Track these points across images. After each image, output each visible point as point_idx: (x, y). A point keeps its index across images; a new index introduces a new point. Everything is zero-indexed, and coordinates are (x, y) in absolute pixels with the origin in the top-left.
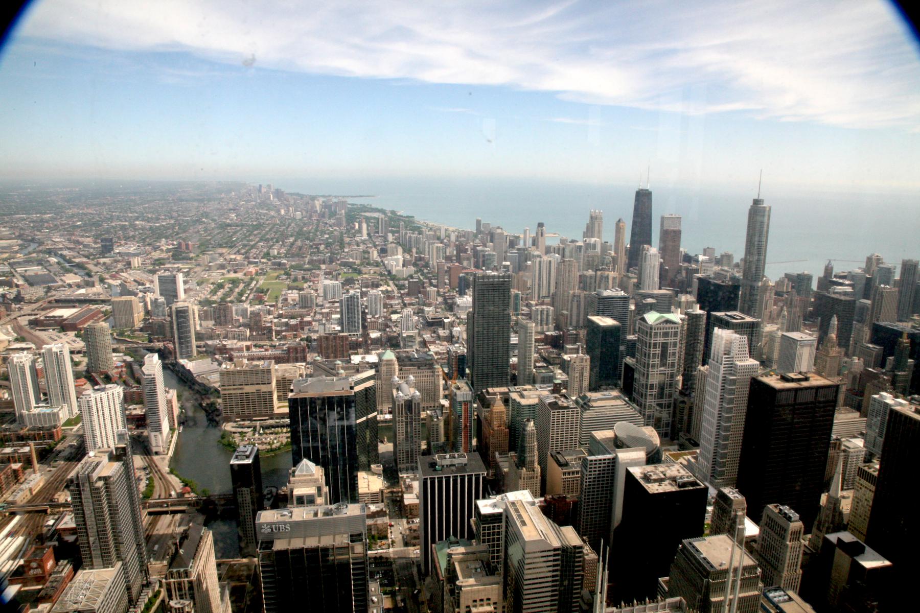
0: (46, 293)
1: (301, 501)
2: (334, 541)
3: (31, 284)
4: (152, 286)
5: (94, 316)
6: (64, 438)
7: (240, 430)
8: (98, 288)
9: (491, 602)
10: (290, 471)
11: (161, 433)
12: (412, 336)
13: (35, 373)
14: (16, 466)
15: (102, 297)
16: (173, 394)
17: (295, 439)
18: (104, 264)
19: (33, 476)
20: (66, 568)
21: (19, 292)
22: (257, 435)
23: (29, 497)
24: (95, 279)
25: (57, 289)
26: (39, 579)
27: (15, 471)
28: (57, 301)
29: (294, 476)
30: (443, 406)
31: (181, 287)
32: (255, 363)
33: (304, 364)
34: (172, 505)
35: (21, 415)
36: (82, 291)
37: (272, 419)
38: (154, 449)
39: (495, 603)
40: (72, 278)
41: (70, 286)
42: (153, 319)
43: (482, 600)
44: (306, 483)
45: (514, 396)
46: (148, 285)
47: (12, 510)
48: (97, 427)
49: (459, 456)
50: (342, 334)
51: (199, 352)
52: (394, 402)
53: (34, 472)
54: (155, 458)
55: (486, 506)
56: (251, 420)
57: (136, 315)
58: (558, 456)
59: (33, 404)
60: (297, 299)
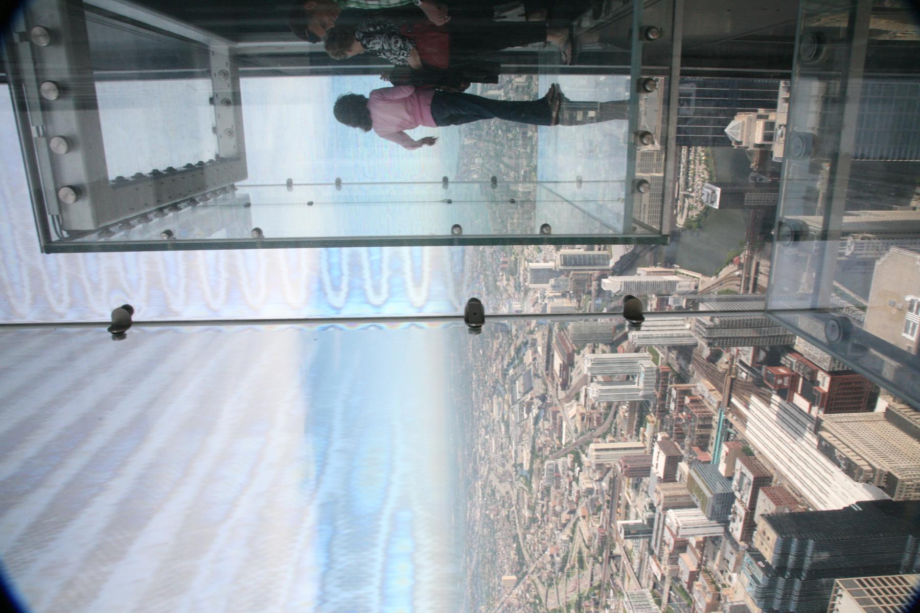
0: (539, 377)
1: (769, 137)
3: (531, 388)
4: (539, 292)
5: (562, 341)
6: (668, 364)
7: (685, 211)
8: (538, 336)
10: (736, 147)
11: (678, 282)
13: (608, 381)
14: (687, 400)
15: (546, 333)
16: (640, 270)
17: (704, 143)
18: (517, 330)
19: (699, 388)
20: (789, 359)
21: (537, 397)
22: (693, 194)
23: (717, 392)
24: (529, 338)
25: (536, 369)
26: (794, 379)
27: (692, 401)
28: (547, 369)
29: (740, 143)
31: (542, 265)
34: (749, 274)
35: (643, 396)
36: (540, 349)
37: (679, 179)
38: (693, 289)
40: (528, 357)
41: (534, 359)
42: (570, 289)
44: (750, 132)
46: (538, 295)
47: (726, 403)
48: (663, 333)
53: (695, 387)
54: (700, 288)
56: (677, 199)
57: (565, 305)
59: (635, 386)
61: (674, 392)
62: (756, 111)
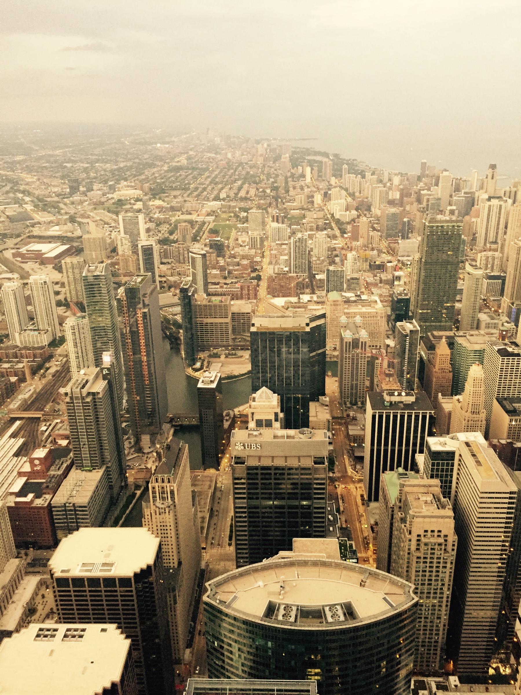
2: (299, 462)
9: (442, 534)
12: (356, 279)
30: (388, 346)
32: (213, 298)
33: (255, 301)
39: (446, 536)
43: (433, 531)
45: (460, 340)
49: (407, 394)
50: (290, 275)
51: (161, 287)
52: (342, 339)
55: (436, 443)
58: (504, 402)
60: (247, 240)
61: (20, 365)
62: (282, 411)
